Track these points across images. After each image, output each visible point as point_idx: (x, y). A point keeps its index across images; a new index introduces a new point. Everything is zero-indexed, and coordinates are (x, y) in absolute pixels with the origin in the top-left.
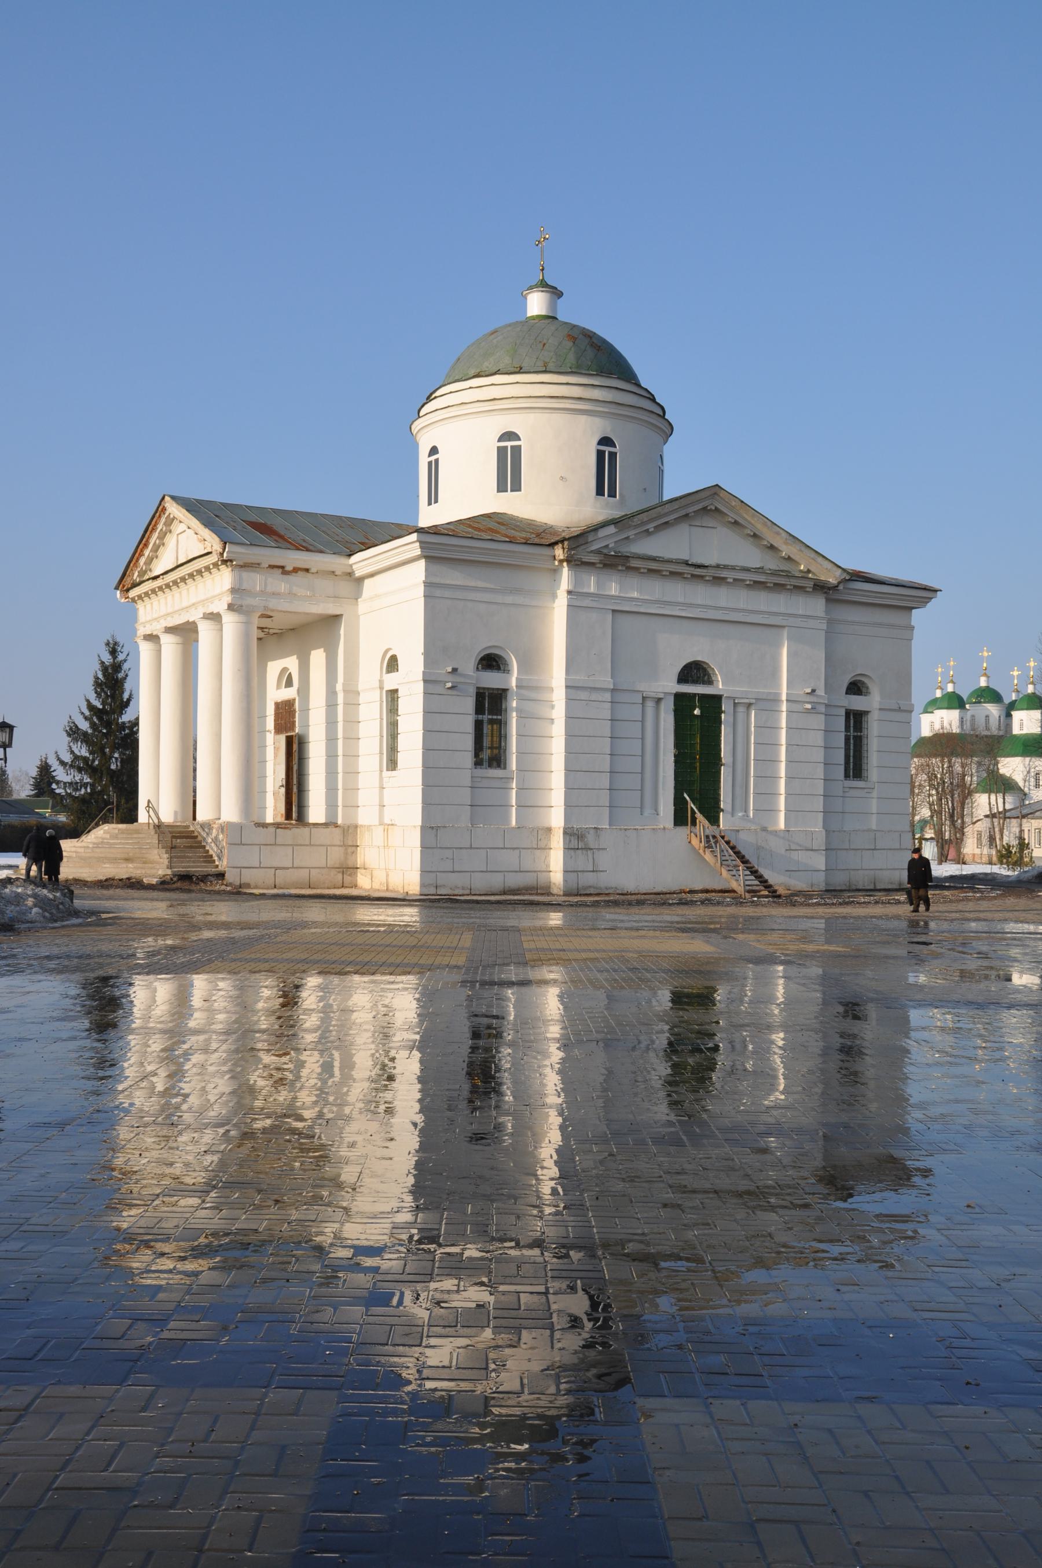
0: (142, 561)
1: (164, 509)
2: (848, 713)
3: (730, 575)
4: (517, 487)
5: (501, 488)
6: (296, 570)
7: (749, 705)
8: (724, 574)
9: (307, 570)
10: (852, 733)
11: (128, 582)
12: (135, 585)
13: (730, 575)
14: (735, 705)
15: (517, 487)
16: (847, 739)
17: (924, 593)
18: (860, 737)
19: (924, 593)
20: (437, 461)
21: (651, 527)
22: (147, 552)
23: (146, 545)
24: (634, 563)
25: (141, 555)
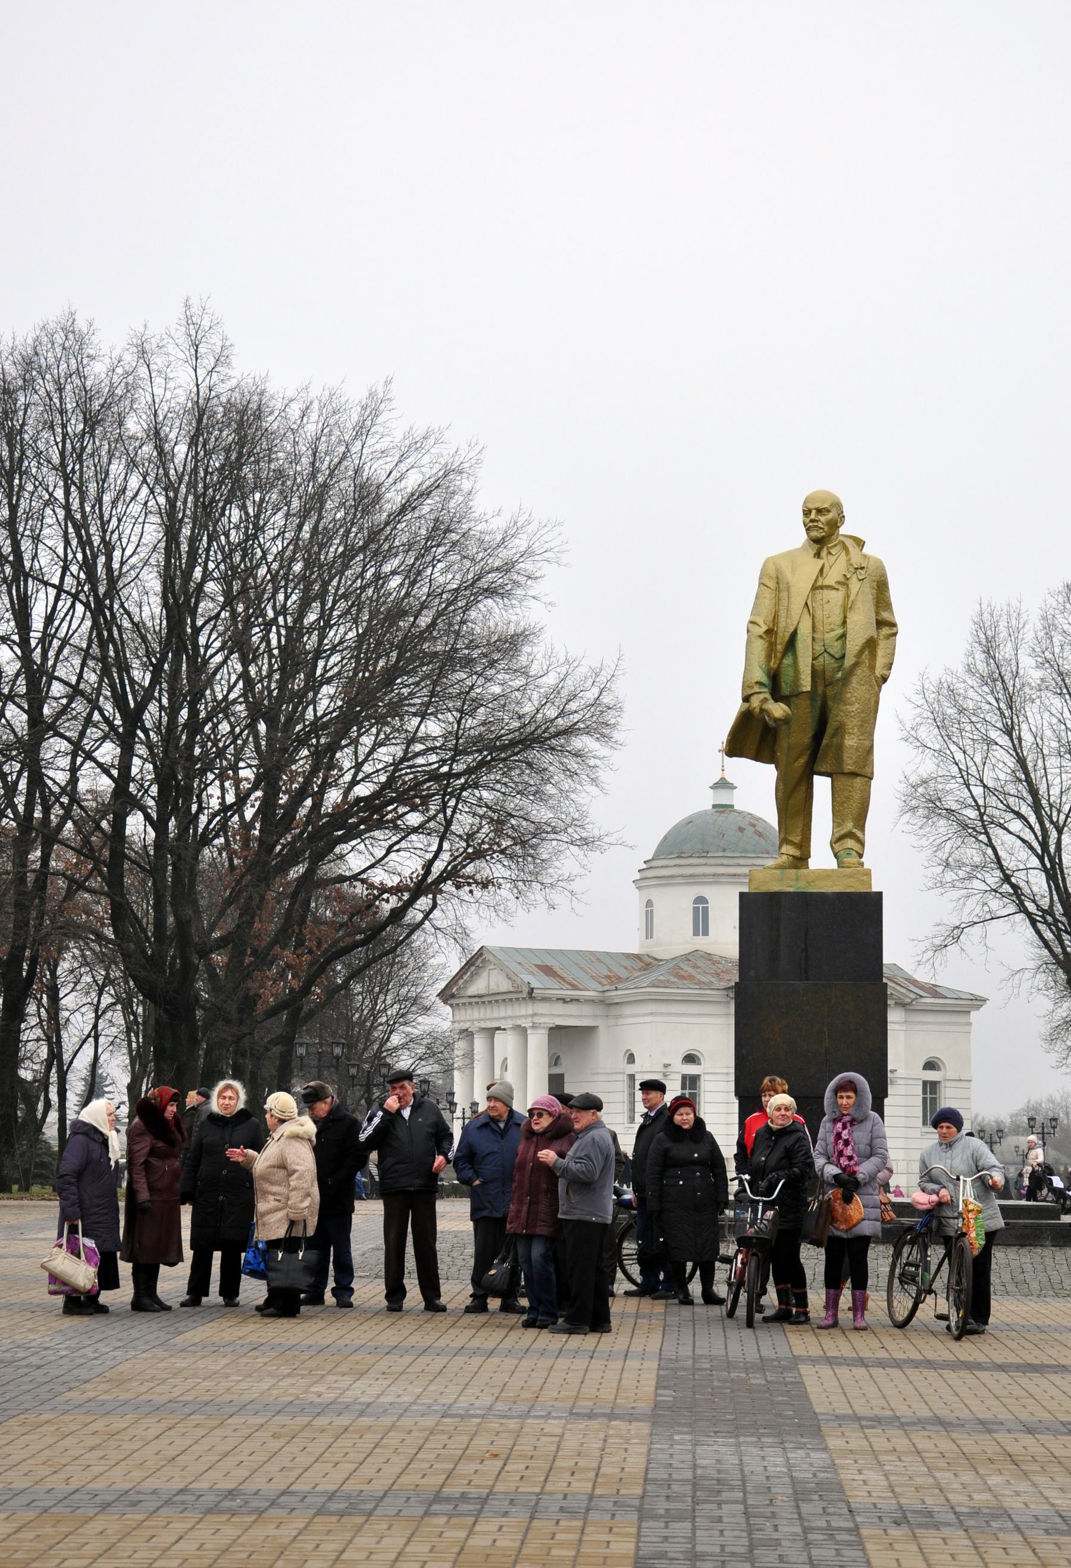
0: (461, 982)
2: (925, 1083)
4: (706, 933)
5: (696, 933)
6: (572, 1000)
9: (578, 1000)
10: (928, 1096)
11: (448, 992)
12: (453, 996)
16: (924, 1100)
17: (978, 1002)
18: (935, 1099)
19: (978, 1002)
20: (652, 911)
22: (465, 977)
23: (465, 973)
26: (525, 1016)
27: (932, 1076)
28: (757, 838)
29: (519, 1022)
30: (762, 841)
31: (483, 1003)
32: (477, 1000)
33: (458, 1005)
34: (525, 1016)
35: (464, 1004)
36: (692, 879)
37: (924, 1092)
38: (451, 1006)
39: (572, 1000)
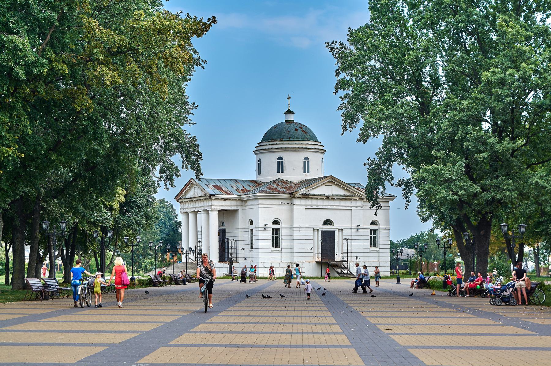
1: (191, 181)
2: (371, 230)
3: (336, 198)
4: (282, 172)
5: (278, 172)
6: (227, 199)
7: (342, 230)
8: (334, 197)
9: (230, 199)
12: (181, 199)
13: (336, 198)
14: (338, 230)
15: (282, 172)
16: (371, 237)
20: (261, 163)
21: (314, 187)
23: (185, 189)
24: (310, 197)
25: (183, 191)
26: (208, 206)
27: (374, 227)
28: (302, 133)
29: (206, 209)
30: (305, 135)
31: (192, 201)
32: (190, 200)
33: (182, 202)
34: (208, 206)
35: (185, 202)
36: (277, 150)
37: (371, 234)
38: (180, 202)
39: (227, 199)
